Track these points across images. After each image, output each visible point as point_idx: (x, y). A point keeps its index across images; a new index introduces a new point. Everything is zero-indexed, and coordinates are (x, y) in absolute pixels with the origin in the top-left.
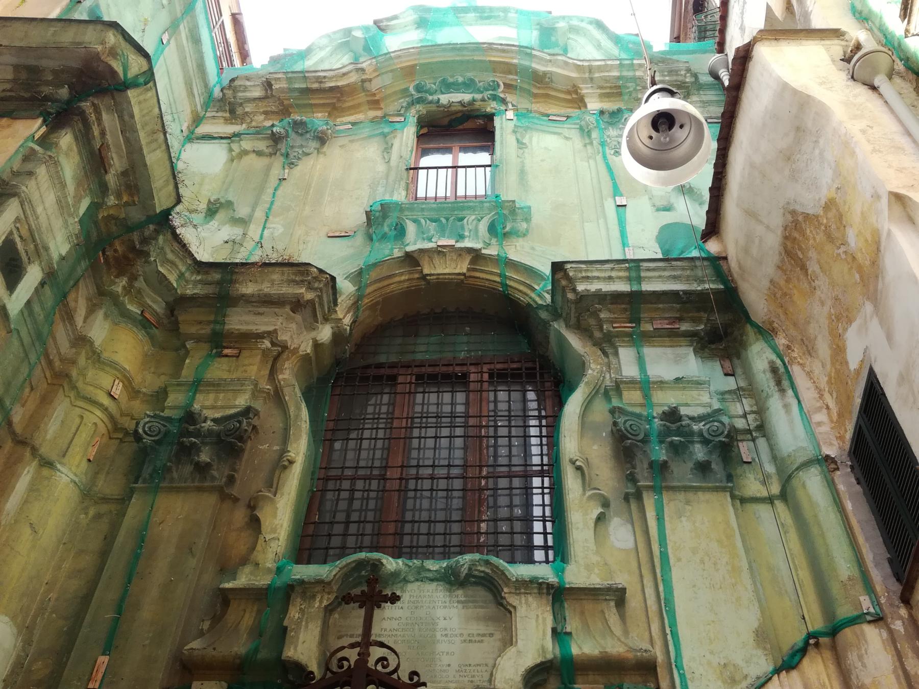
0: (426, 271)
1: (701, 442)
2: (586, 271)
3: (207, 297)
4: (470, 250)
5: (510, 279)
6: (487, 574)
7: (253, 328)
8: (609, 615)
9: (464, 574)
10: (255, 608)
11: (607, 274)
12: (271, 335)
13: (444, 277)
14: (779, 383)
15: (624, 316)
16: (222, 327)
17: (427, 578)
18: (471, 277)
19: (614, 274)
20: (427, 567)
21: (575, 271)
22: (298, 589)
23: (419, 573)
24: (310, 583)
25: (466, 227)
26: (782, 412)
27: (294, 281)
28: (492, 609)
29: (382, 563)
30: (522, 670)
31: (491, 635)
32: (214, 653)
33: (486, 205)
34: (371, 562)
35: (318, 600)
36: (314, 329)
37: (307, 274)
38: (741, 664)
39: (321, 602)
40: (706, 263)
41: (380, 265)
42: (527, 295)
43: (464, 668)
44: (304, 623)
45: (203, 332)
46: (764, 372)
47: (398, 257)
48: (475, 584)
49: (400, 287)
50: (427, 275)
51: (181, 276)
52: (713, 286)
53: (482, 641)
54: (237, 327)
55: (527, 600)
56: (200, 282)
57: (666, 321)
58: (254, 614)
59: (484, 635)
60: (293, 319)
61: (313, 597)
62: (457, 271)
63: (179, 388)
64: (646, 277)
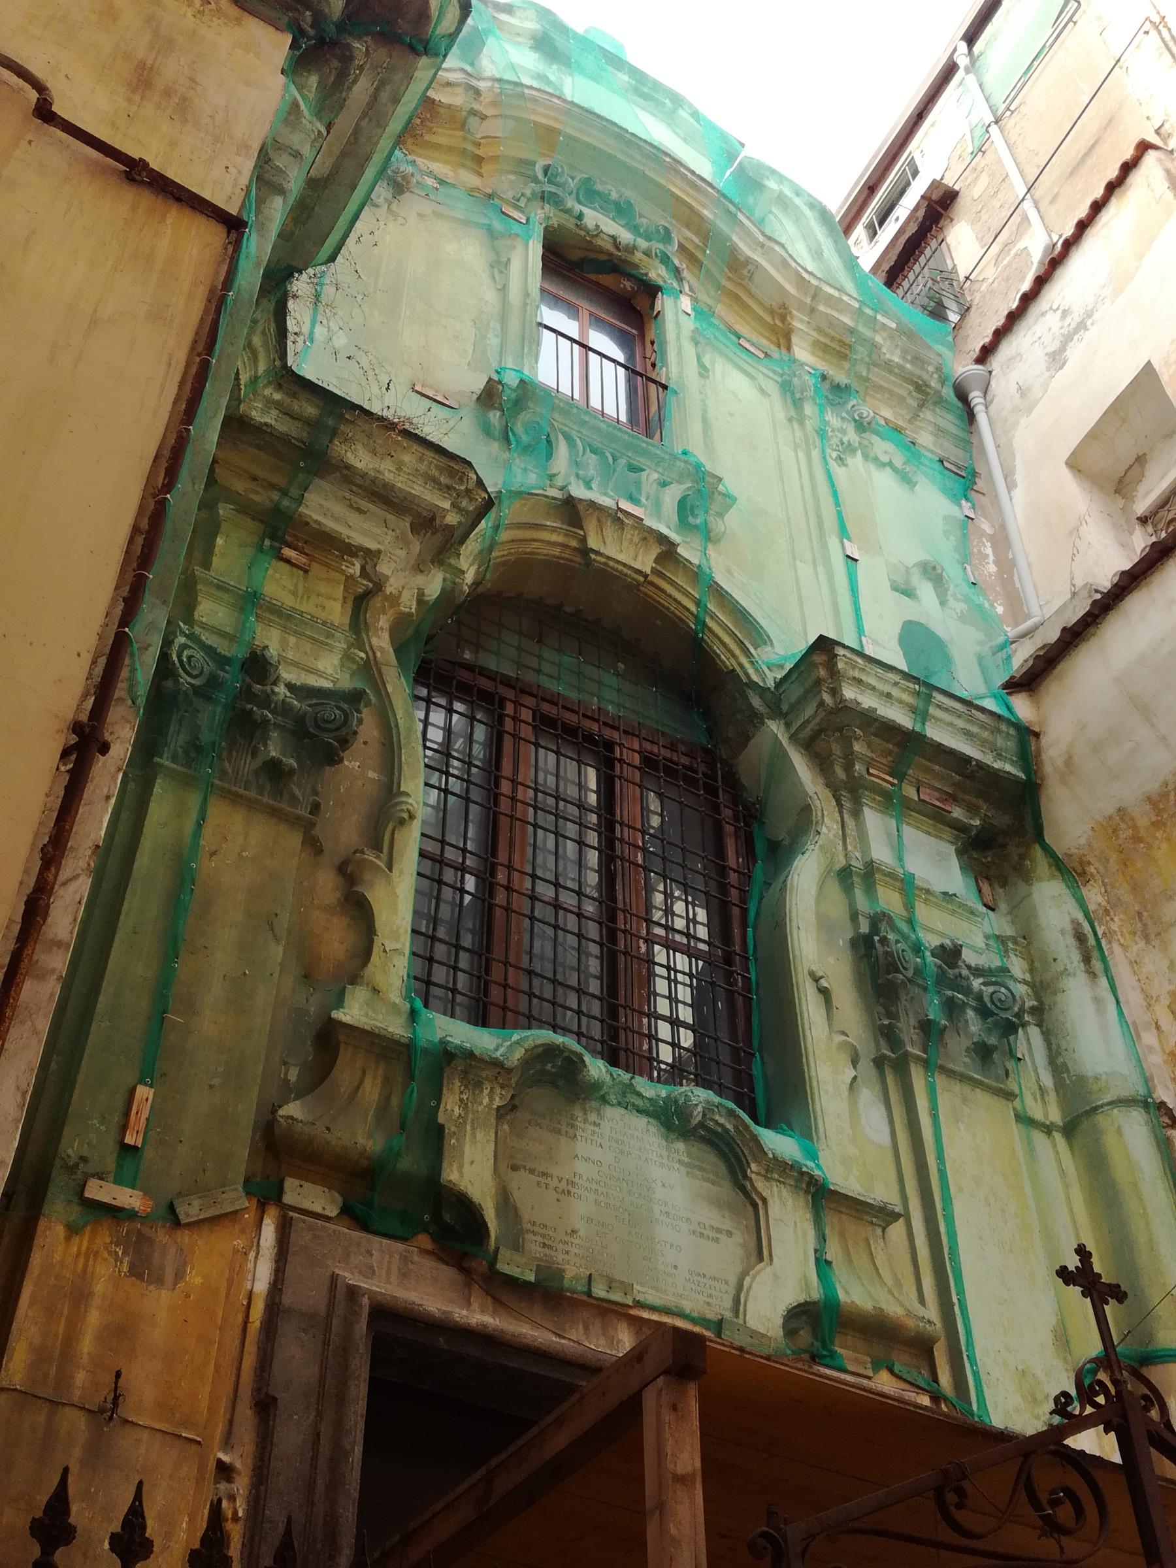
0: (592, 543)
1: (975, 1009)
2: (862, 670)
3: (285, 439)
4: (662, 539)
5: (712, 617)
6: (727, 1131)
7: (344, 531)
8: (876, 1249)
9: (696, 1122)
10: (381, 1072)
11: (886, 688)
12: (371, 556)
13: (616, 566)
14: (1087, 959)
15: (884, 761)
16: (294, 506)
17: (634, 1105)
18: (652, 584)
19: (895, 692)
20: (638, 1089)
21: (846, 663)
22: (459, 1064)
23: (624, 1094)
24: (481, 1060)
25: (644, 486)
26: (1090, 1008)
27: (434, 480)
28: (726, 1190)
29: (583, 1062)
30: (781, 1310)
31: (729, 1234)
32: (328, 1136)
33: (678, 463)
34: (566, 1054)
35: (486, 1092)
36: (421, 571)
37: (461, 479)
38: (1041, 1376)
39: (491, 1099)
40: (1012, 731)
41: (524, 499)
42: (734, 656)
43: (696, 1278)
44: (468, 1128)
45: (256, 498)
46: (1063, 932)
47: (555, 499)
48: (703, 1139)
49: (546, 552)
50: (593, 551)
51: (254, 380)
52: (1008, 768)
53: (717, 1240)
54: (315, 517)
55: (780, 1192)
56: (278, 405)
57: (937, 794)
58: (379, 1081)
59: (719, 1231)
60: (407, 543)
61: (478, 1085)
62: (637, 566)
63: (219, 594)
64: (937, 719)
